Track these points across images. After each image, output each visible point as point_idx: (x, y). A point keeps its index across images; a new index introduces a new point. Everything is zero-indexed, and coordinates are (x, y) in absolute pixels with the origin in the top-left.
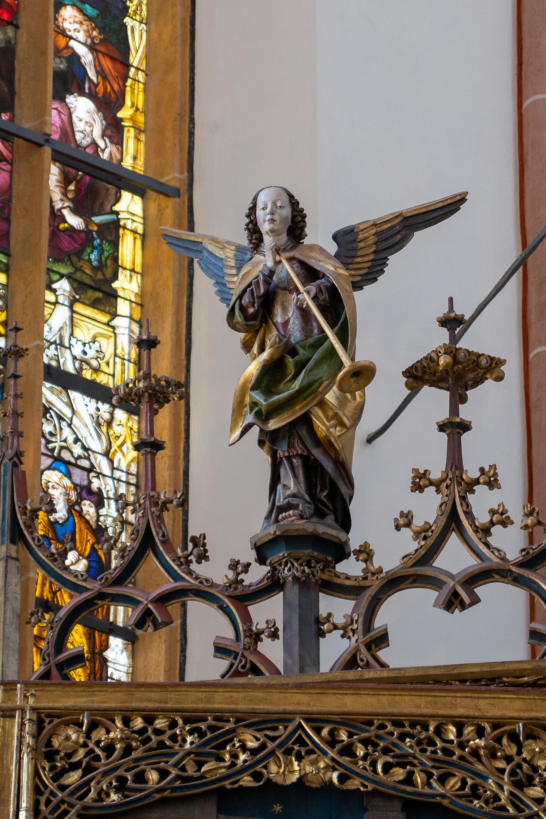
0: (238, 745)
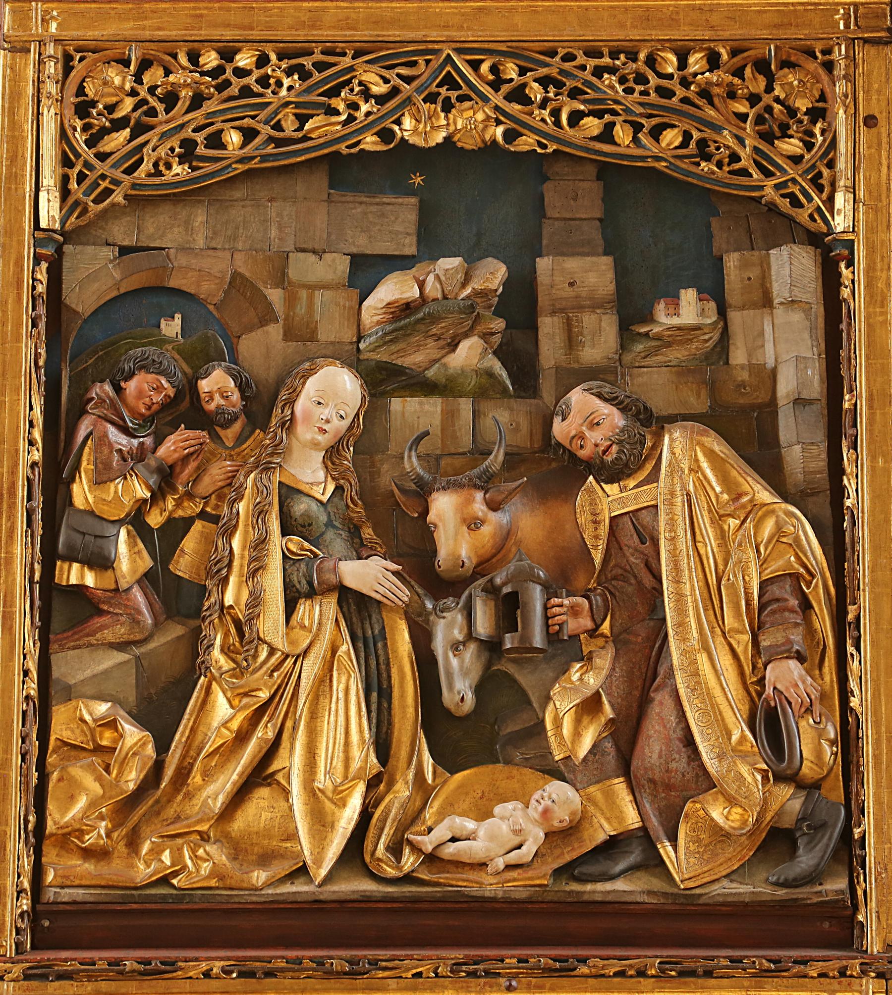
0: (357, 89)
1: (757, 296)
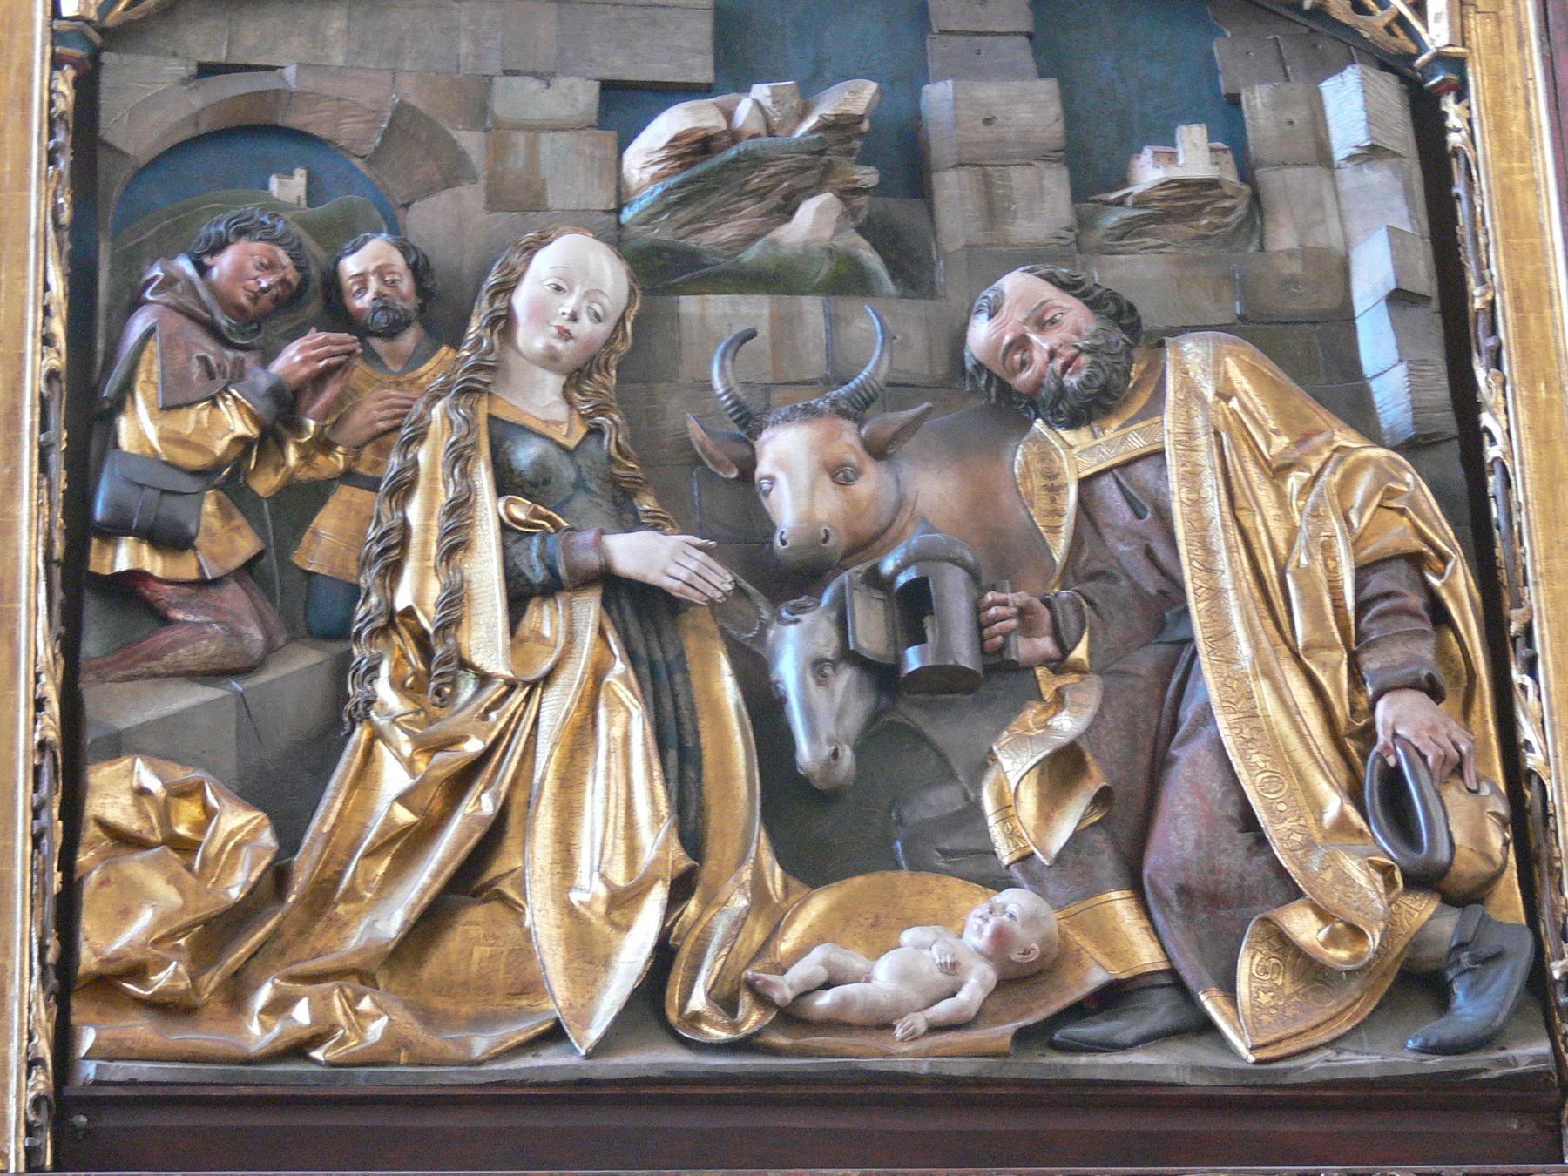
1: (1305, 147)
